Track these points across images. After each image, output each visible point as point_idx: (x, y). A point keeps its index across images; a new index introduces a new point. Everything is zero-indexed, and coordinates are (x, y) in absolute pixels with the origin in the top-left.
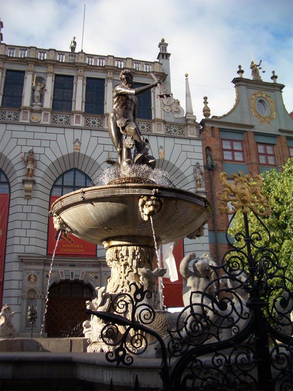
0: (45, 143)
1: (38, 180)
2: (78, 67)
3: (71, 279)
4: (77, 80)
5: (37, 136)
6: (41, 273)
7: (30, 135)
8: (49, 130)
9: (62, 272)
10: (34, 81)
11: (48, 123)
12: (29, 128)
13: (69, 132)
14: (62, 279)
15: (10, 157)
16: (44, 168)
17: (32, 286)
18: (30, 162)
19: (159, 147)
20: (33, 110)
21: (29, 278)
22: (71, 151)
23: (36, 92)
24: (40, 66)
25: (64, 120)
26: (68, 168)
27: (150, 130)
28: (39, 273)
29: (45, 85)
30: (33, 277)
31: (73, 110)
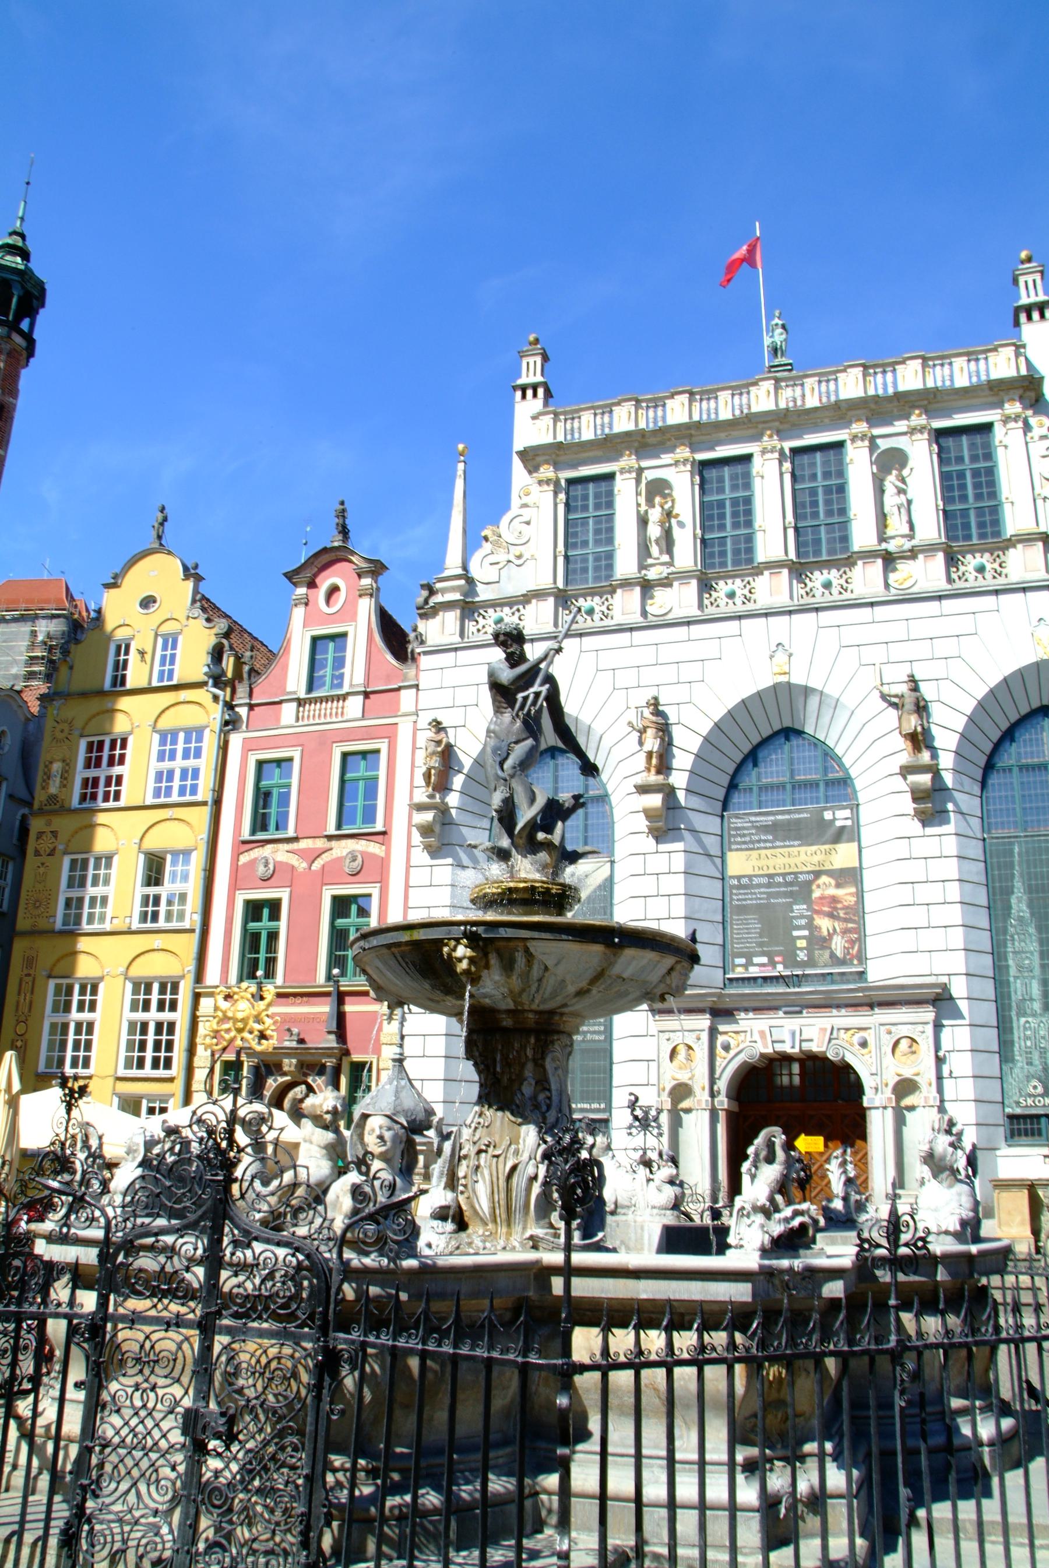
0: (689, 672)
1: (679, 779)
2: (760, 426)
3: (789, 1050)
5: (667, 653)
6: (705, 1036)
7: (647, 655)
9: (762, 1033)
11: (694, 612)
15: (598, 728)
16: (695, 744)
17: (684, 1077)
19: (1035, 623)
22: (766, 681)
26: (766, 732)
27: (1004, 571)
28: (699, 1039)
29: (673, 501)
30: (682, 1050)
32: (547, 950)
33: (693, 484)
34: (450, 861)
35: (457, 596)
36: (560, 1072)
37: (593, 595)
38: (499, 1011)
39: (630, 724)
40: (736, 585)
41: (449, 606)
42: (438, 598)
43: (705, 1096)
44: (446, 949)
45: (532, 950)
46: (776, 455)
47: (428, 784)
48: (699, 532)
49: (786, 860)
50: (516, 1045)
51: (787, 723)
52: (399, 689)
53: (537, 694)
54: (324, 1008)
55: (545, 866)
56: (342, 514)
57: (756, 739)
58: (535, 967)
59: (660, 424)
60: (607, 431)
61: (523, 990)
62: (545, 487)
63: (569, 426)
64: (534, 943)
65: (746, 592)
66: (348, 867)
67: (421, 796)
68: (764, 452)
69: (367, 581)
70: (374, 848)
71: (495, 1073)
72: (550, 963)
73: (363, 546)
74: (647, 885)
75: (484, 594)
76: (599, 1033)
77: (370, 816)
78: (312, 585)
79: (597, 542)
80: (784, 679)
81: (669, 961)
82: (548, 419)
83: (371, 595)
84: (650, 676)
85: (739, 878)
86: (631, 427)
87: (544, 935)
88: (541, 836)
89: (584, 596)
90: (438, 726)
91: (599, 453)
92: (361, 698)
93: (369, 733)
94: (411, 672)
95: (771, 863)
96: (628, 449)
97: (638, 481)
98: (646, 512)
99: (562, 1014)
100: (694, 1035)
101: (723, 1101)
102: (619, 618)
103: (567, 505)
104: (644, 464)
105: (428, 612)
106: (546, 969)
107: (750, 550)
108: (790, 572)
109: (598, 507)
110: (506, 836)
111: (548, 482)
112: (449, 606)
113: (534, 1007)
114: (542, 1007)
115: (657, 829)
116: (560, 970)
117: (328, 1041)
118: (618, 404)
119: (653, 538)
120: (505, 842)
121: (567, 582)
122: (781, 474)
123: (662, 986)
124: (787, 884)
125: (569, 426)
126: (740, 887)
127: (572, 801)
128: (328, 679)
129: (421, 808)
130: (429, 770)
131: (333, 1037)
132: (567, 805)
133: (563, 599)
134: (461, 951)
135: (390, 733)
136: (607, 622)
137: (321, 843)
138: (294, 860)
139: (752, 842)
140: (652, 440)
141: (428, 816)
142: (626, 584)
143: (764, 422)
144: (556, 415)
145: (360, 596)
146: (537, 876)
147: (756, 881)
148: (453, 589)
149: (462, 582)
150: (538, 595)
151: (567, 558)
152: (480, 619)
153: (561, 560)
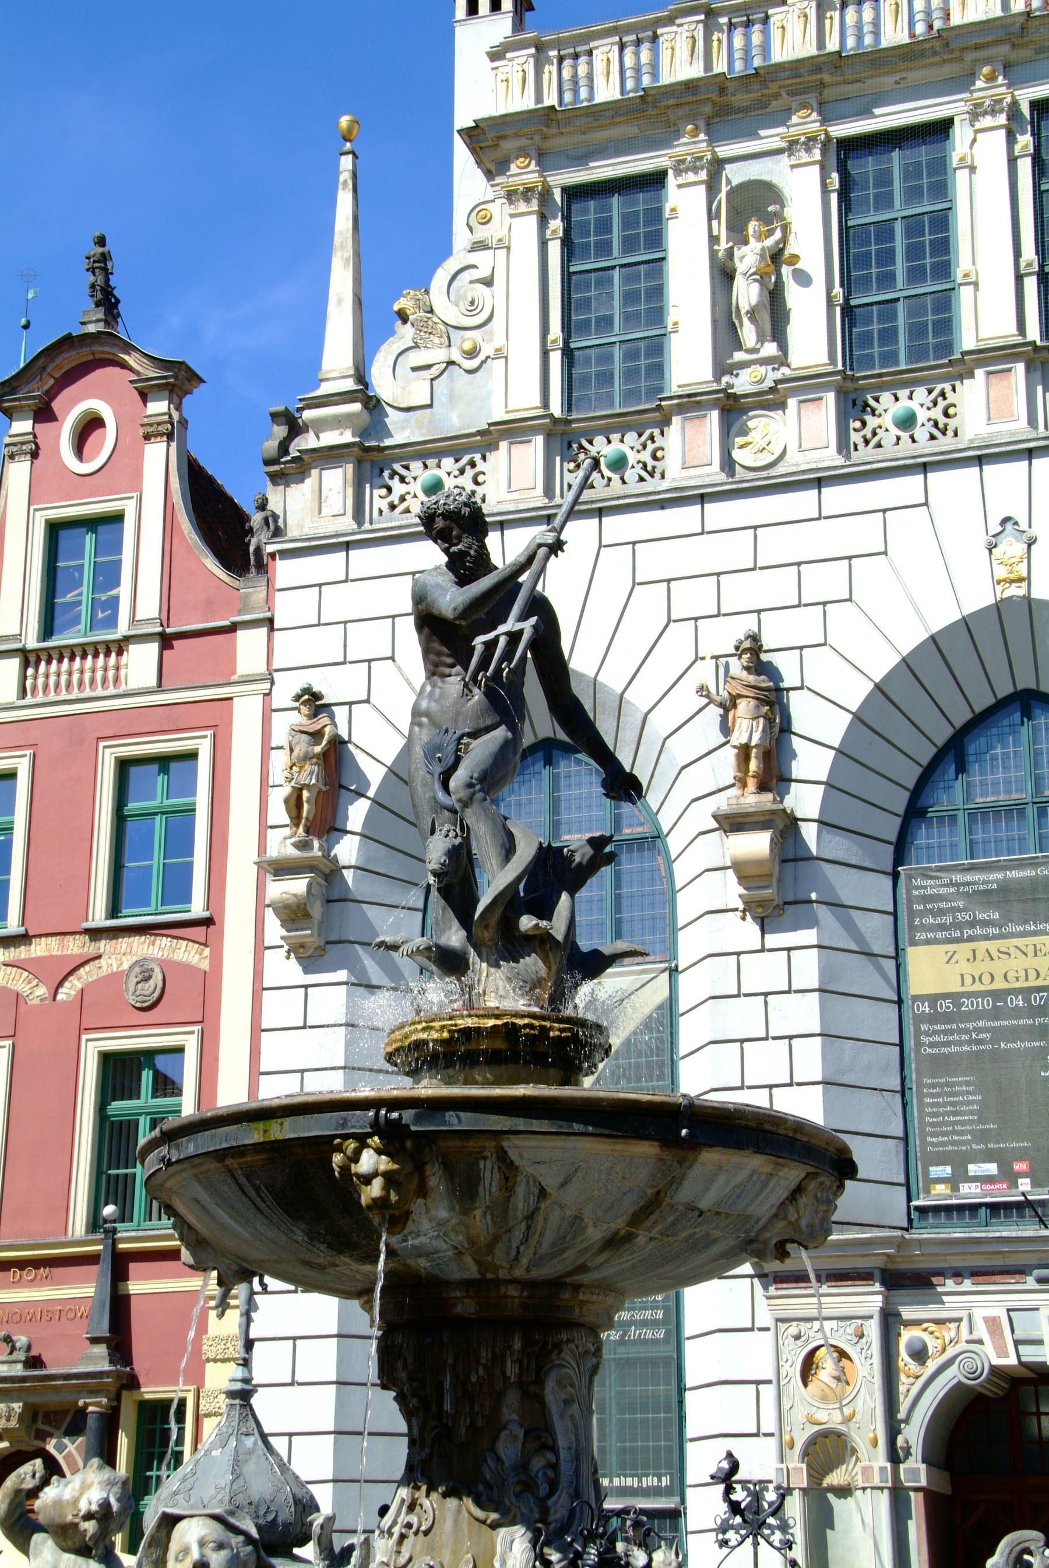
1: (805, 801)
2: (969, 56)
4: (974, 140)
5: (776, 546)
6: (873, 1330)
7: (735, 550)
8: (836, 497)
9: (992, 1323)
10: (718, 217)
11: (830, 457)
12: (718, 513)
13: (952, 486)
14: (996, 1361)
15: (639, 698)
16: (834, 727)
17: (830, 1417)
18: (745, 707)
20: (735, 397)
21: (808, 1367)
22: (979, 597)
23: (739, 282)
24: (745, 110)
25: (922, 416)
26: (983, 701)
29: (785, 228)
31: (967, 341)
32: (543, 1156)
33: (825, 191)
34: (342, 975)
35: (347, 437)
36: (575, 1408)
37: (623, 430)
38: (447, 1284)
39: (702, 690)
40: (917, 401)
41: (331, 456)
42: (309, 441)
43: (880, 1460)
44: (337, 1158)
45: (513, 1155)
46: (1002, 119)
47: (296, 820)
48: (838, 290)
49: (1030, 962)
50: (485, 1355)
51: (1026, 681)
52: (233, 628)
53: (514, 637)
54: (84, 1289)
55: (537, 983)
56: (102, 264)
57: (961, 716)
58: (521, 1191)
59: (757, 62)
60: (646, 81)
61: (496, 1239)
62: (522, 207)
63: (566, 74)
64: (516, 1141)
65: (937, 413)
66: (134, 993)
67: (282, 844)
68: (975, 114)
69: (158, 407)
70: (186, 953)
71: (440, 1414)
72: (550, 1182)
73: (154, 331)
74: (745, 1018)
75: (402, 431)
76: (654, 1324)
77: (178, 886)
78: (44, 414)
79: (630, 319)
80: (1017, 591)
81: (793, 1174)
82: (523, 59)
83: (170, 436)
84: (739, 592)
85: (933, 999)
86: (695, 71)
87: (536, 1125)
88: (527, 922)
89: (606, 432)
90: (313, 701)
91: (630, 130)
92: (154, 647)
93: (173, 720)
94: (259, 594)
95: (998, 967)
96: (690, 118)
97: (712, 188)
98: (730, 253)
99: (577, 1288)
100: (851, 1327)
101: (916, 1471)
102: (675, 474)
103: (567, 242)
104: (724, 151)
105: (287, 468)
106: (543, 1193)
107: (946, 326)
108: (1028, 370)
109: (629, 245)
110: (456, 924)
111: (527, 193)
112: (331, 456)
113: (519, 1273)
114: (535, 1273)
115: (762, 903)
116: (571, 1196)
117: (93, 1359)
118: (670, 21)
119: (744, 307)
120: (455, 937)
121: (569, 403)
122: (1012, 161)
123: (780, 1224)
124: (1034, 1011)
125: (566, 74)
126: (935, 1018)
127: (589, 851)
128: (85, 609)
129: (282, 869)
130: (298, 791)
131: (101, 1350)
132: (577, 858)
133: (563, 438)
134: (368, 1161)
135: (217, 720)
136: (652, 485)
137: (76, 946)
138: (19, 982)
139: (958, 926)
140: (740, 99)
141: (297, 886)
142: (691, 403)
143: (977, 47)
144: (540, 48)
145: (147, 437)
146: (521, 1004)
147: (967, 1005)
148: (338, 422)
149: (357, 407)
150: (512, 430)
151: (568, 353)
152: (395, 484)
153: (556, 359)
